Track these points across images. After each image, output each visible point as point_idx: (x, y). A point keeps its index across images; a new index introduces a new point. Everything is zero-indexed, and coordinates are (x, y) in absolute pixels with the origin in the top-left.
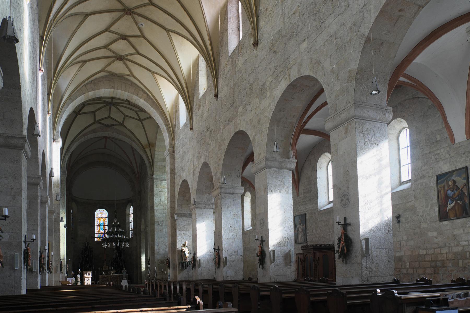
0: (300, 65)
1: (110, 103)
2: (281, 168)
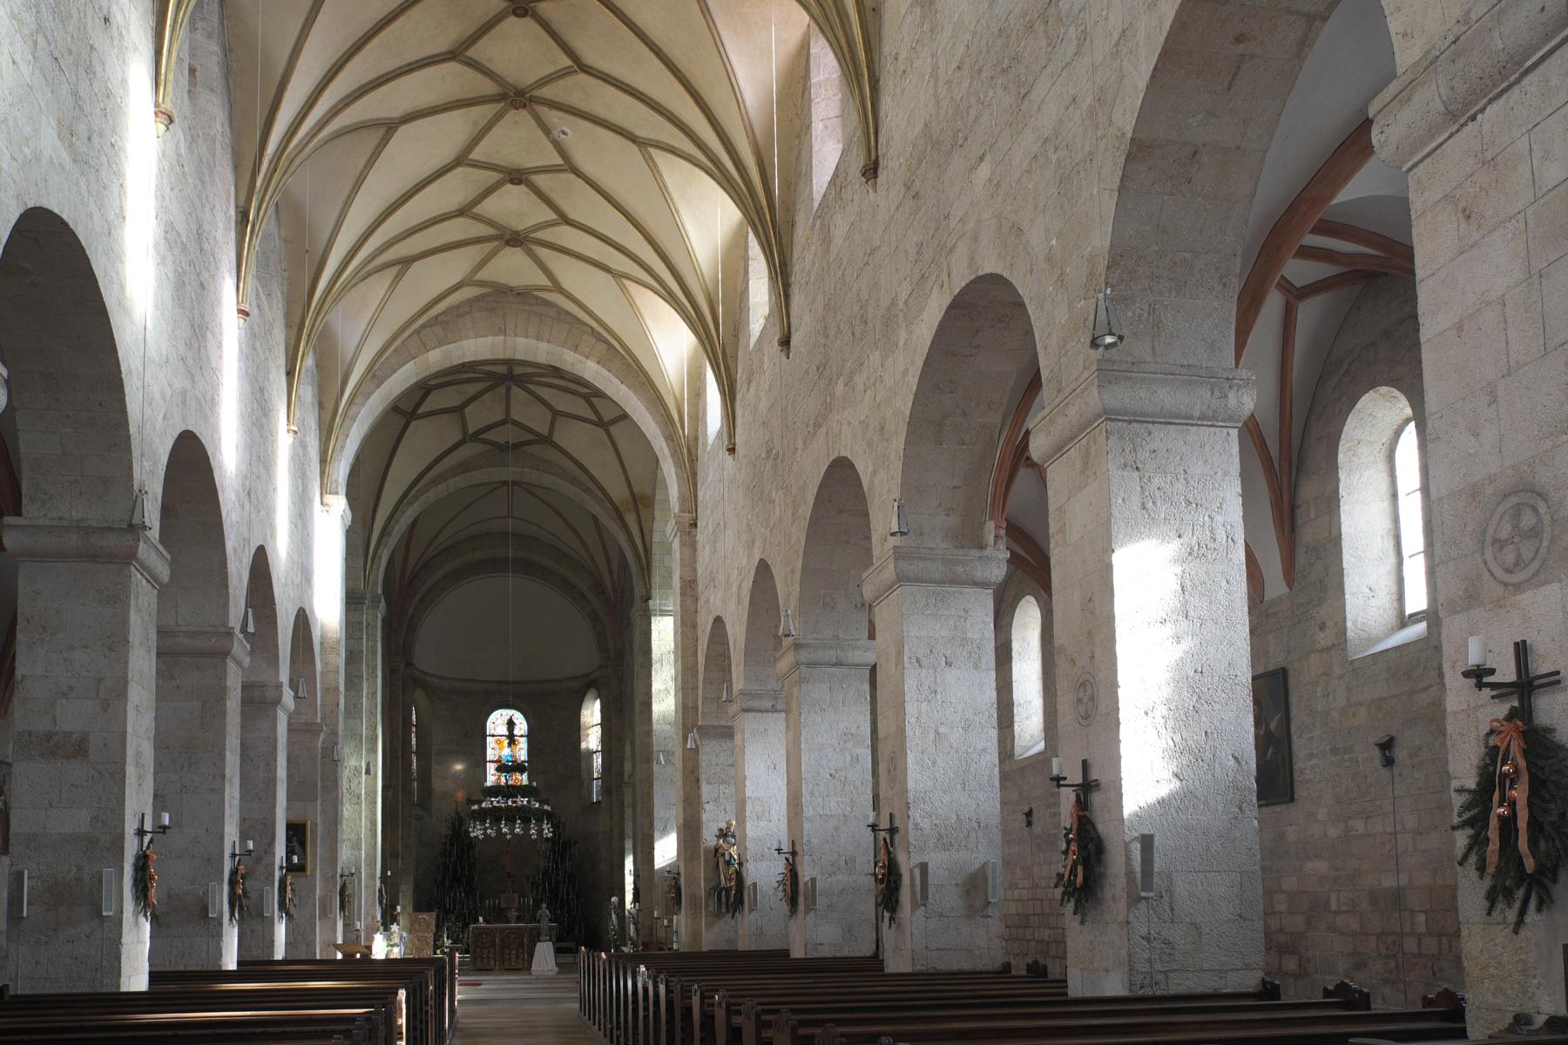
0: (975, 239)
1: (506, 377)
2: (952, 582)
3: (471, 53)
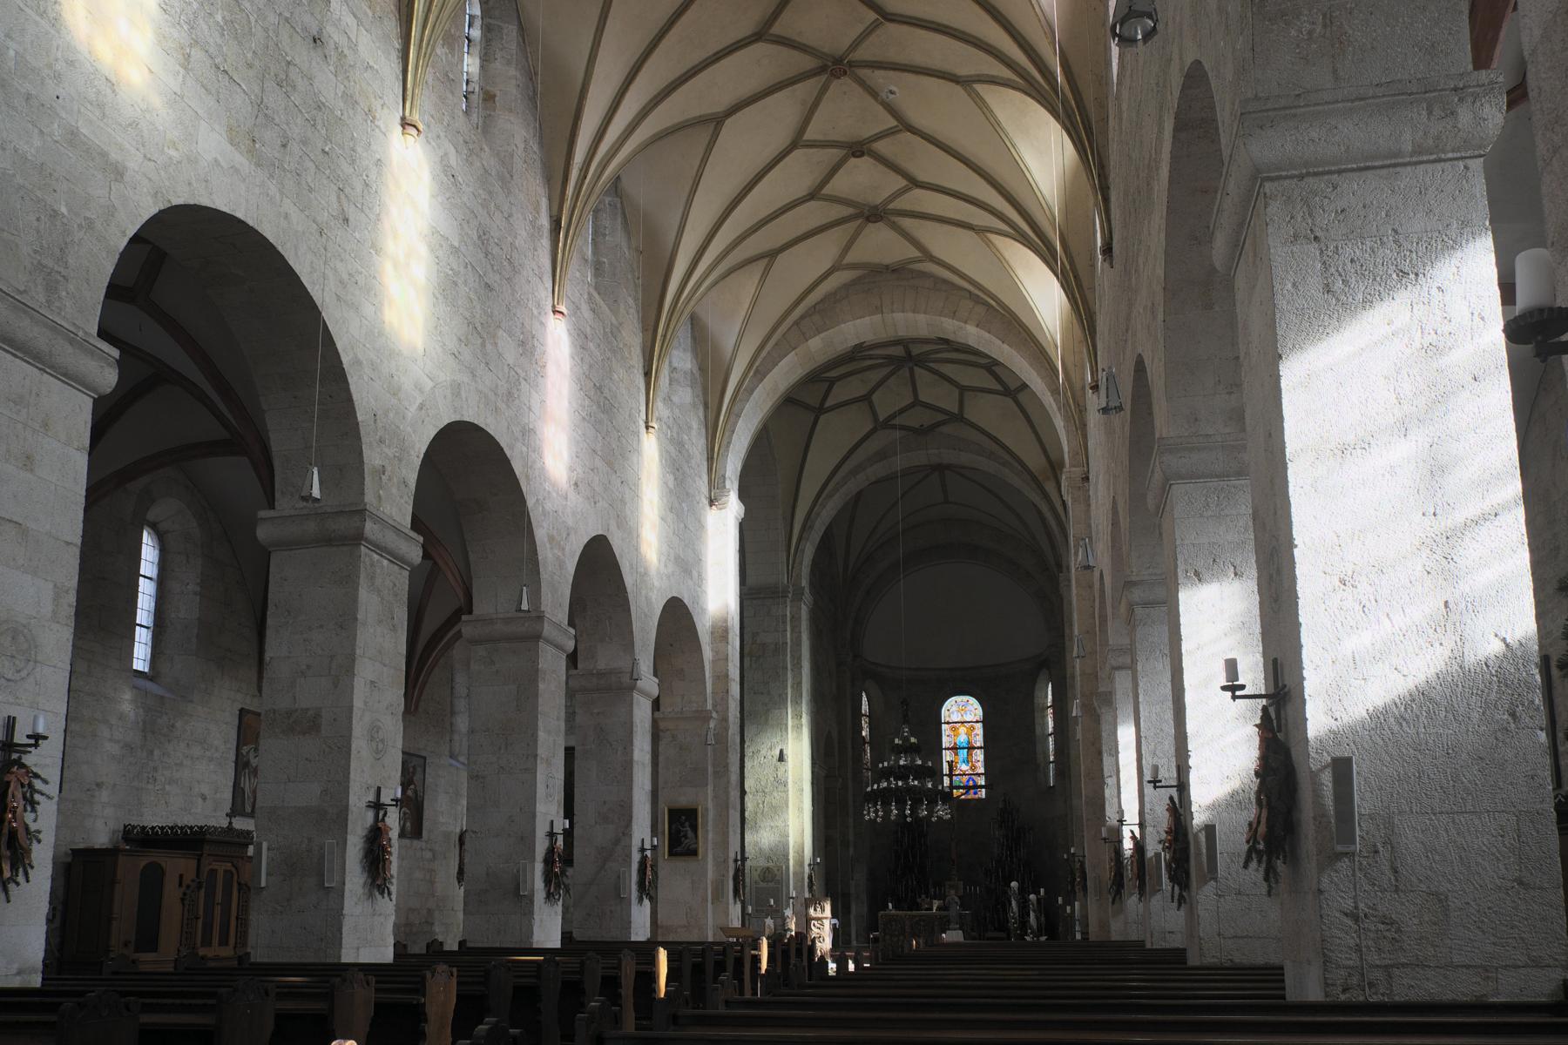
1: (907, 357)
3: (776, 29)
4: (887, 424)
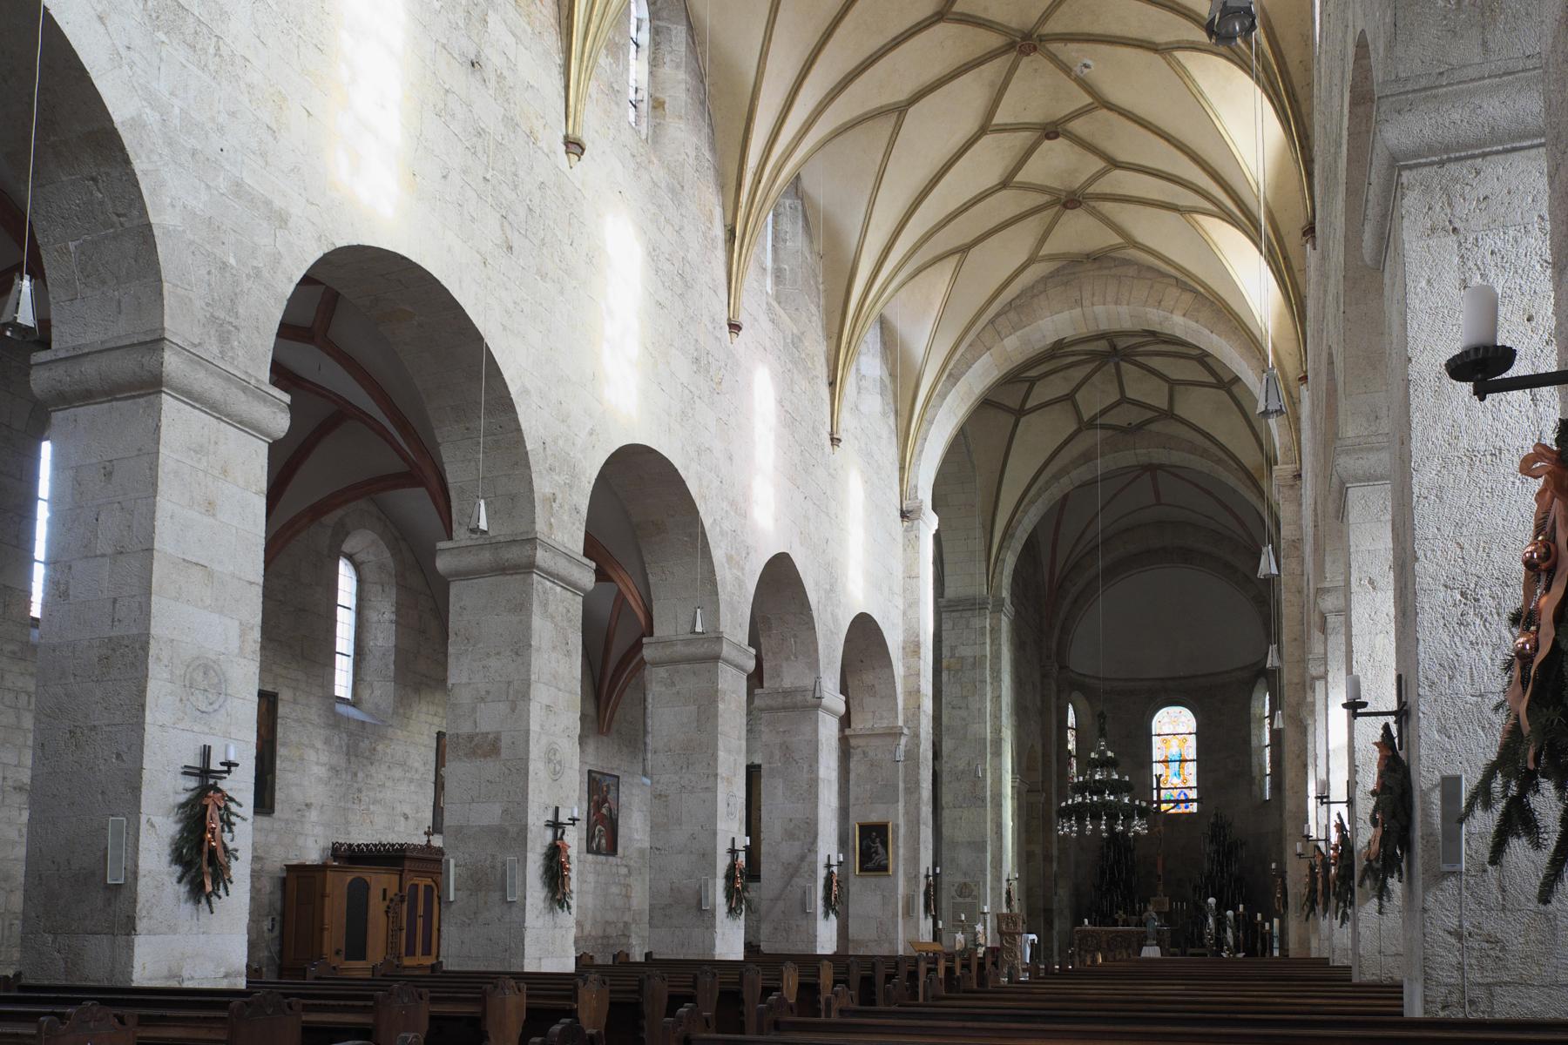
1: (1112, 352)
4: (1091, 424)
